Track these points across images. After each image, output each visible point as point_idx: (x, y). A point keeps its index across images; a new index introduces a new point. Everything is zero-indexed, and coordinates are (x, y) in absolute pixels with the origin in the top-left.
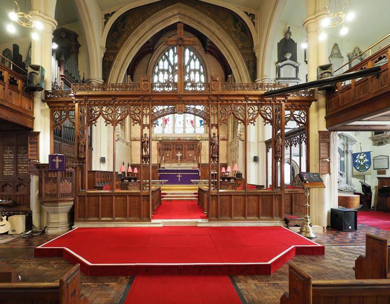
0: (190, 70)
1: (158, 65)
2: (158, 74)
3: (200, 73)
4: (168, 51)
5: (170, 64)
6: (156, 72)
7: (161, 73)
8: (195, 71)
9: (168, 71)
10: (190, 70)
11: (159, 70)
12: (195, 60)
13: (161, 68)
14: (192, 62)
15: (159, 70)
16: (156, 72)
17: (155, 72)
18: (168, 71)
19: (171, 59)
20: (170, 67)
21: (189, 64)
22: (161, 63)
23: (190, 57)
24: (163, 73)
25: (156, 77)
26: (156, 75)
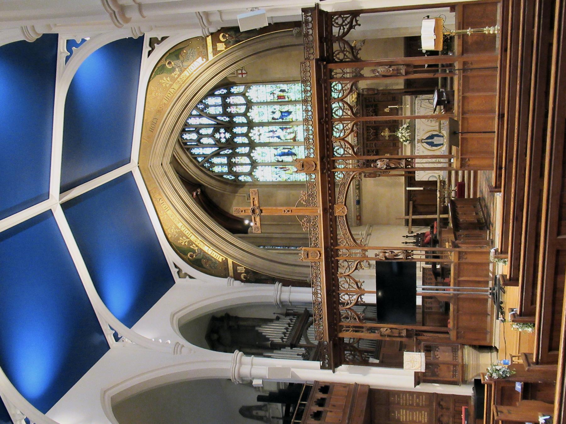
0: (225, 113)
1: (221, 175)
2: (237, 175)
3: (229, 94)
4: (195, 157)
5: (217, 154)
6: (233, 178)
7: (234, 169)
8: (225, 105)
9: (229, 157)
10: (225, 113)
11: (230, 172)
12: (207, 106)
13: (225, 169)
14: (212, 111)
15: (230, 172)
16: (233, 178)
17: (234, 181)
18: (229, 157)
19: (208, 151)
20: (222, 153)
21: (214, 117)
22: (217, 169)
23: (200, 116)
24: (235, 164)
25: (242, 178)
26: (240, 178)
